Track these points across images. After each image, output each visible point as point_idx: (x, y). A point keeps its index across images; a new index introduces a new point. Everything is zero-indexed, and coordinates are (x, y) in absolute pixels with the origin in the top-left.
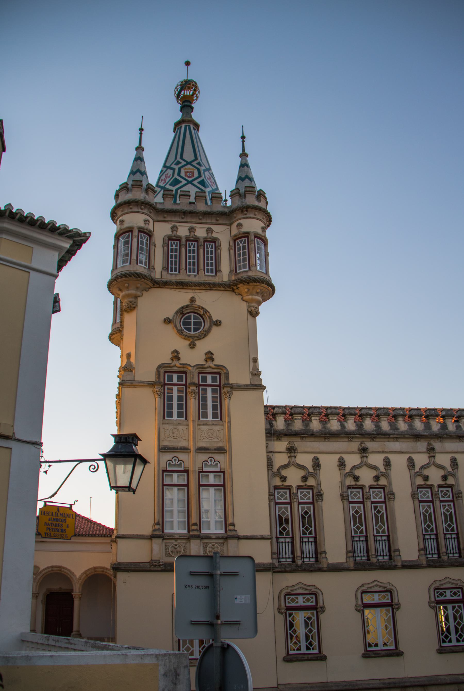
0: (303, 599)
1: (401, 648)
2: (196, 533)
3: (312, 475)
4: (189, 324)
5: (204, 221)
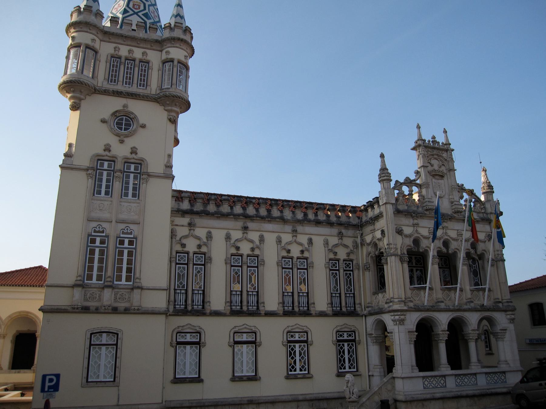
2: (109, 284)
3: (205, 244)
4: (122, 124)
5: (141, 45)
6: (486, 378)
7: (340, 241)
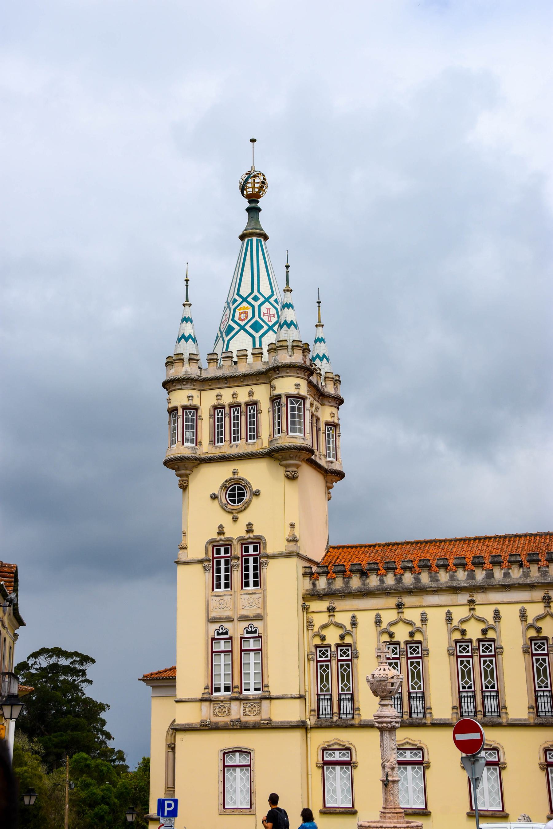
0: (340, 754)
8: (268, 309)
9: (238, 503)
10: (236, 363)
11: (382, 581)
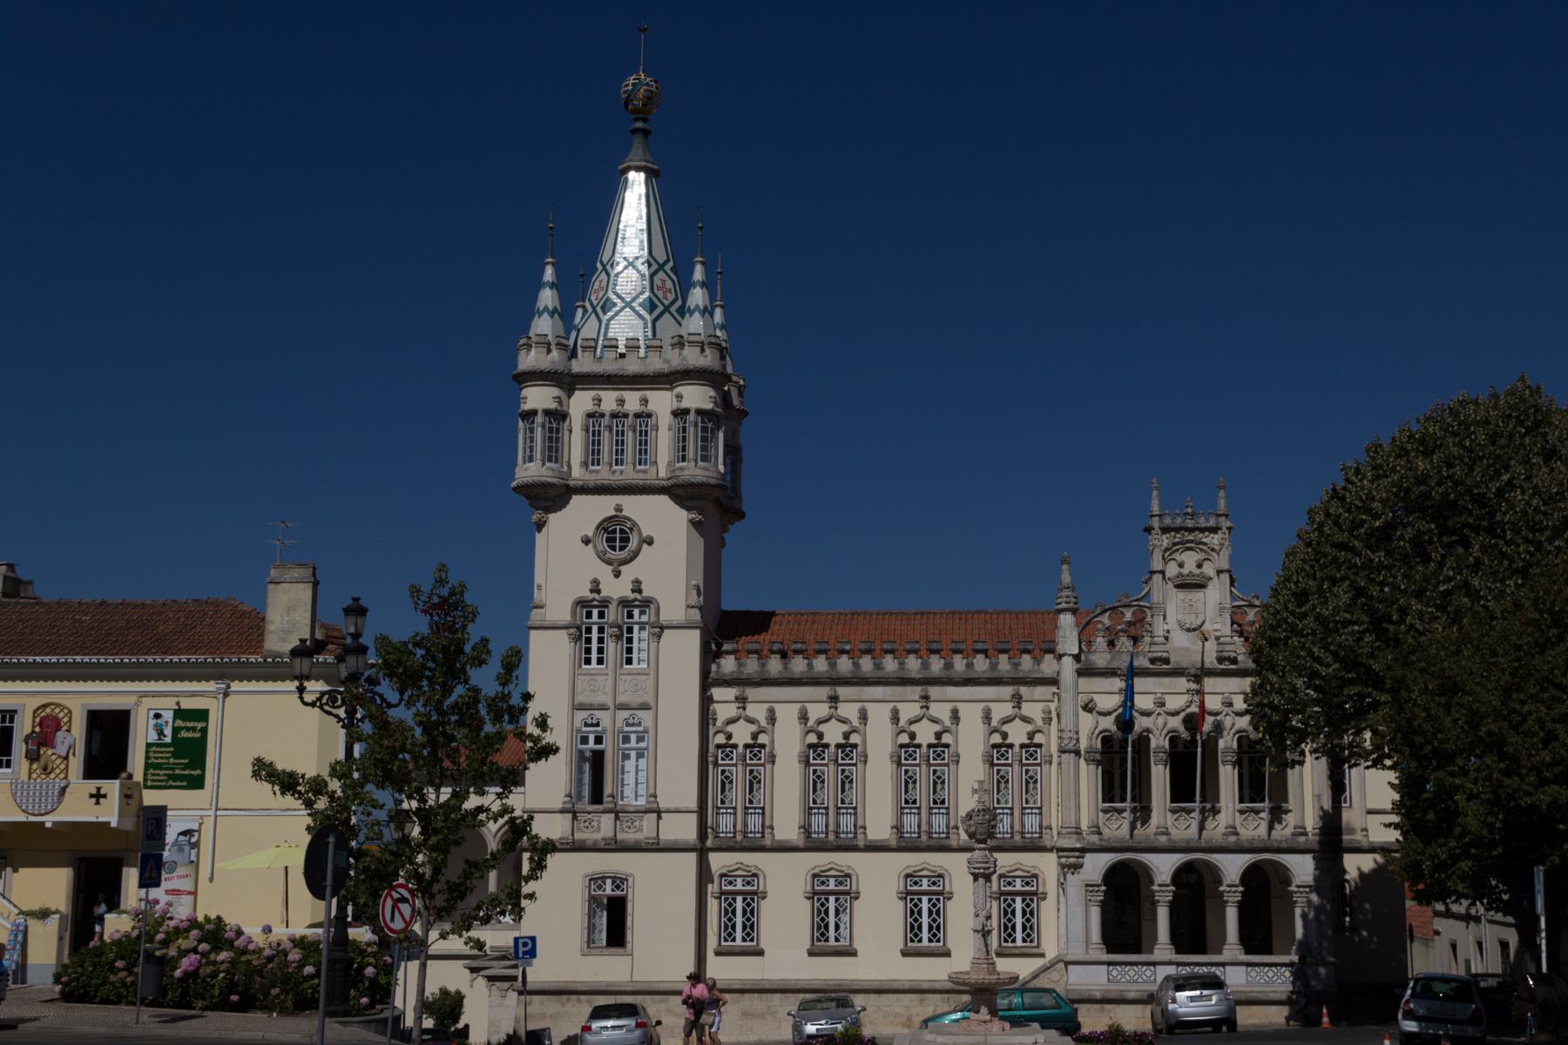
1: (856, 945)
4: (614, 540)
6: (1247, 974)
7: (1016, 710)
8: (664, 281)
9: (620, 550)
10: (622, 356)
11: (810, 666)
